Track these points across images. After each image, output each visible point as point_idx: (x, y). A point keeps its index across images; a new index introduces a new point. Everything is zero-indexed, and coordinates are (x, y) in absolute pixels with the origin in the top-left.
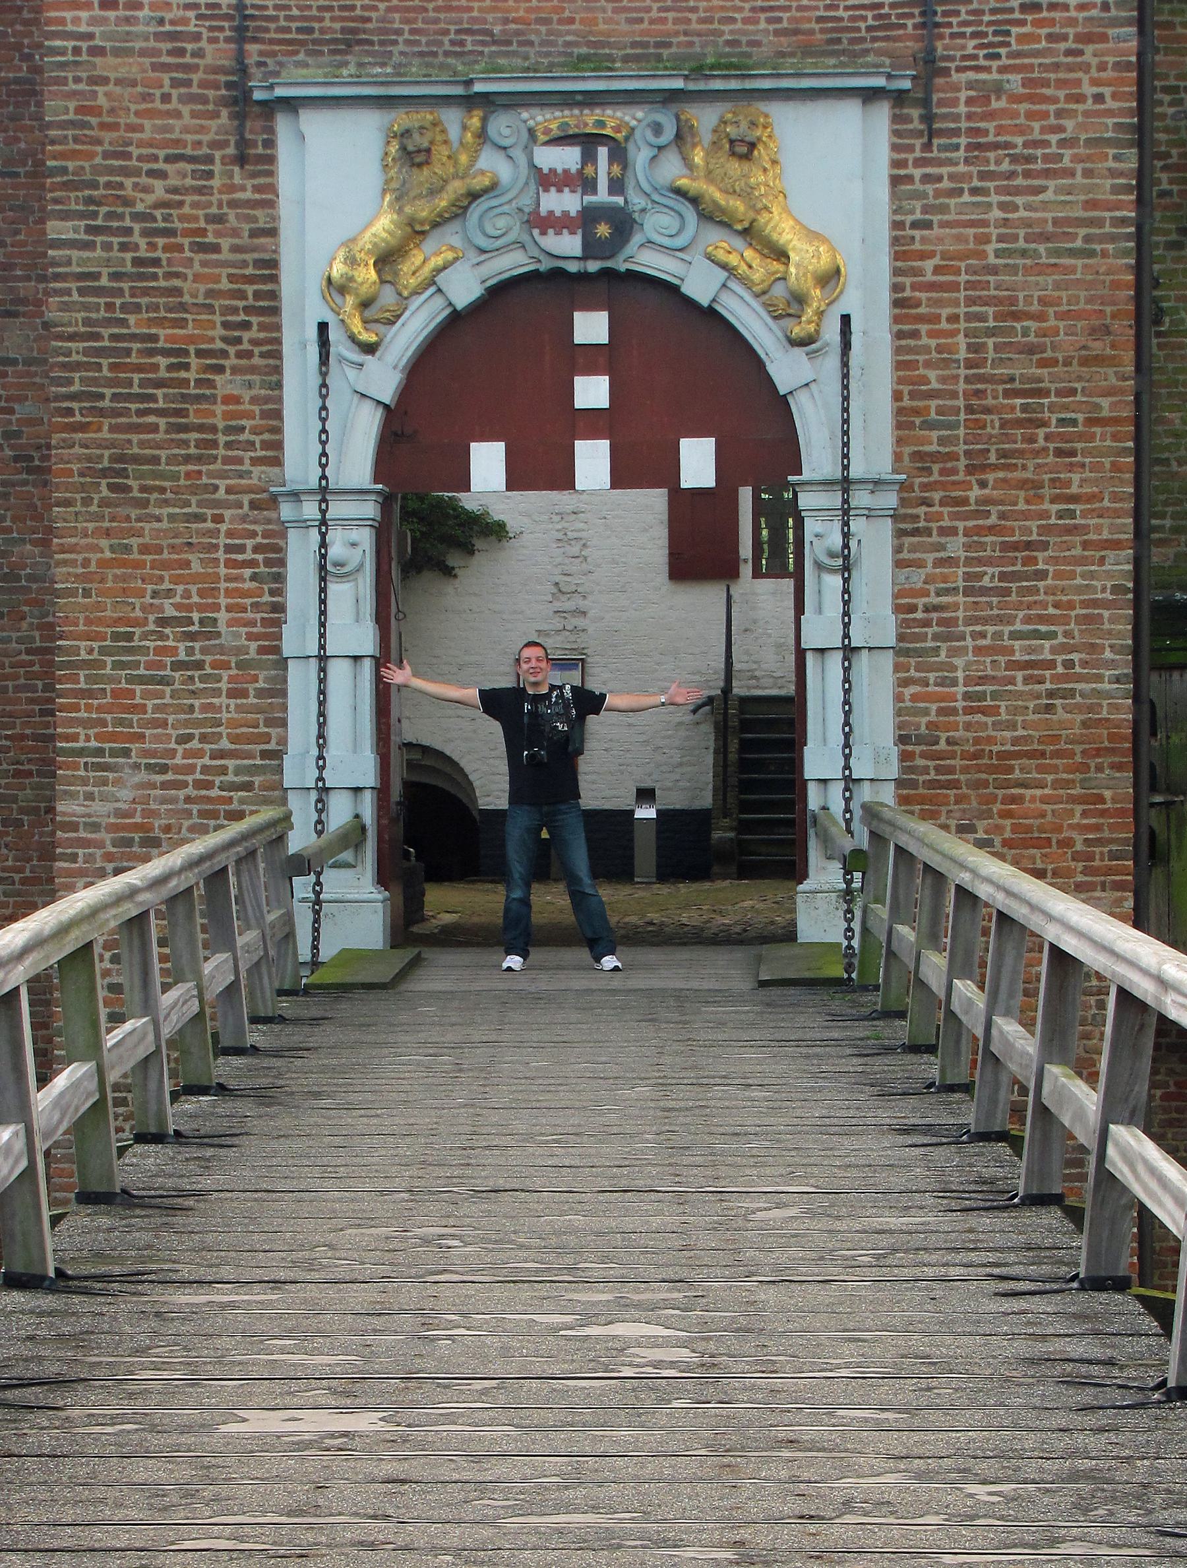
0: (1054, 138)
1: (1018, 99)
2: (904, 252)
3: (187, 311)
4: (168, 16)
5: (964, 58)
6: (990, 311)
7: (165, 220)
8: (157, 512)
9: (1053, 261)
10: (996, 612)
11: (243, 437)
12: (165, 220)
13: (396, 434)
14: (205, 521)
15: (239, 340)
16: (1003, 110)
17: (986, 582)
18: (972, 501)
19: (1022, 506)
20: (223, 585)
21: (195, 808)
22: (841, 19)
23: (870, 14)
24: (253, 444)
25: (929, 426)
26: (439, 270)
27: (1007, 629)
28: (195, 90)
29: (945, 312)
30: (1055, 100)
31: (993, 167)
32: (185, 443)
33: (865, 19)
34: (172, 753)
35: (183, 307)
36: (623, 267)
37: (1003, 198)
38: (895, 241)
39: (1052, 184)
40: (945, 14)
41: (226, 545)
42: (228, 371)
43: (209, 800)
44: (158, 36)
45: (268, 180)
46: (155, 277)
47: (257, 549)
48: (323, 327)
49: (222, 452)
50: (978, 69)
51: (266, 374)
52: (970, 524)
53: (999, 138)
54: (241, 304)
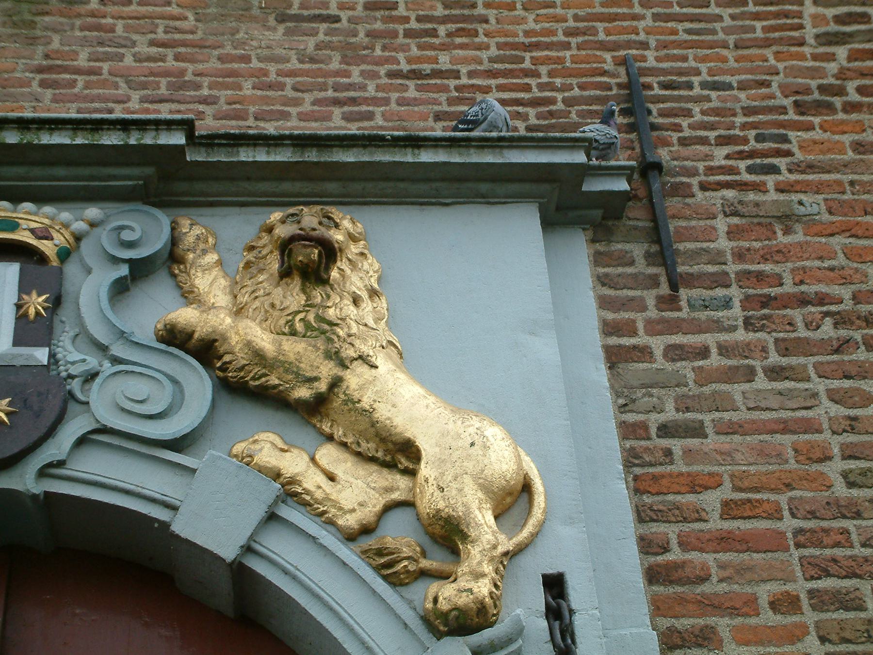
2: (655, 478)
5: (710, 170)
16: (800, 244)
23: (532, 112)
29: (765, 592)
31: (803, 333)
37: (836, 384)
40: (662, 114)
50: (743, 186)
53: (803, 288)
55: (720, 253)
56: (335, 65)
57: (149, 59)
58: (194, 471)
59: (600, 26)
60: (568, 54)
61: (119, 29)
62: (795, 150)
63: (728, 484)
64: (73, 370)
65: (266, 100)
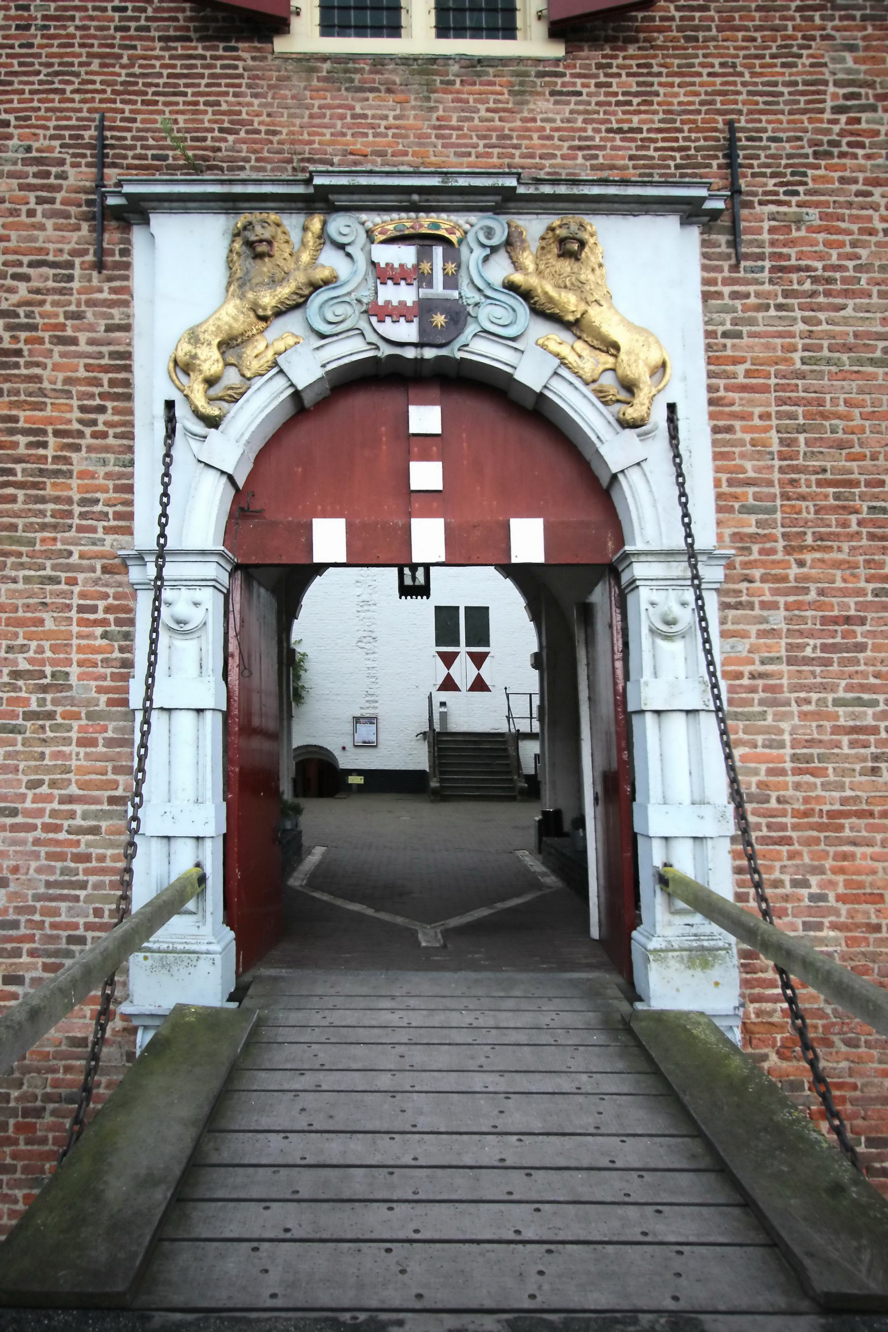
0: (850, 264)
1: (819, 230)
2: (718, 358)
3: (46, 396)
4: (36, 145)
5: (765, 193)
6: (800, 410)
7: (27, 316)
8: (13, 573)
9: (856, 368)
10: (819, 680)
11: (99, 508)
12: (27, 316)
13: (242, 509)
14: (59, 583)
15: (94, 423)
16: (803, 238)
17: (808, 652)
18: (792, 578)
19: (839, 584)
20: (75, 642)
21: (43, 850)
22: (653, 158)
23: (677, 155)
24: (107, 514)
25: (747, 510)
27: (830, 697)
28: (58, 206)
29: (757, 411)
30: (849, 232)
31: (796, 287)
32: (42, 513)
34: (23, 798)
35: (42, 393)
36: (459, 355)
38: (709, 347)
39: (850, 303)
40: (746, 157)
41: (79, 606)
42: (84, 449)
43: (58, 842)
44: (26, 162)
45: (125, 283)
46: (17, 366)
47: (107, 610)
49: (76, 521)
51: (120, 453)
52: (791, 599)
53: (800, 262)
54: (96, 390)
55: (763, 242)
56: (579, 124)
57: (487, 120)
58: (523, 352)
59: (718, 99)
60: (699, 117)
61: (471, 101)
62: (809, 180)
63: (749, 362)
64: (470, 302)
65: (543, 146)
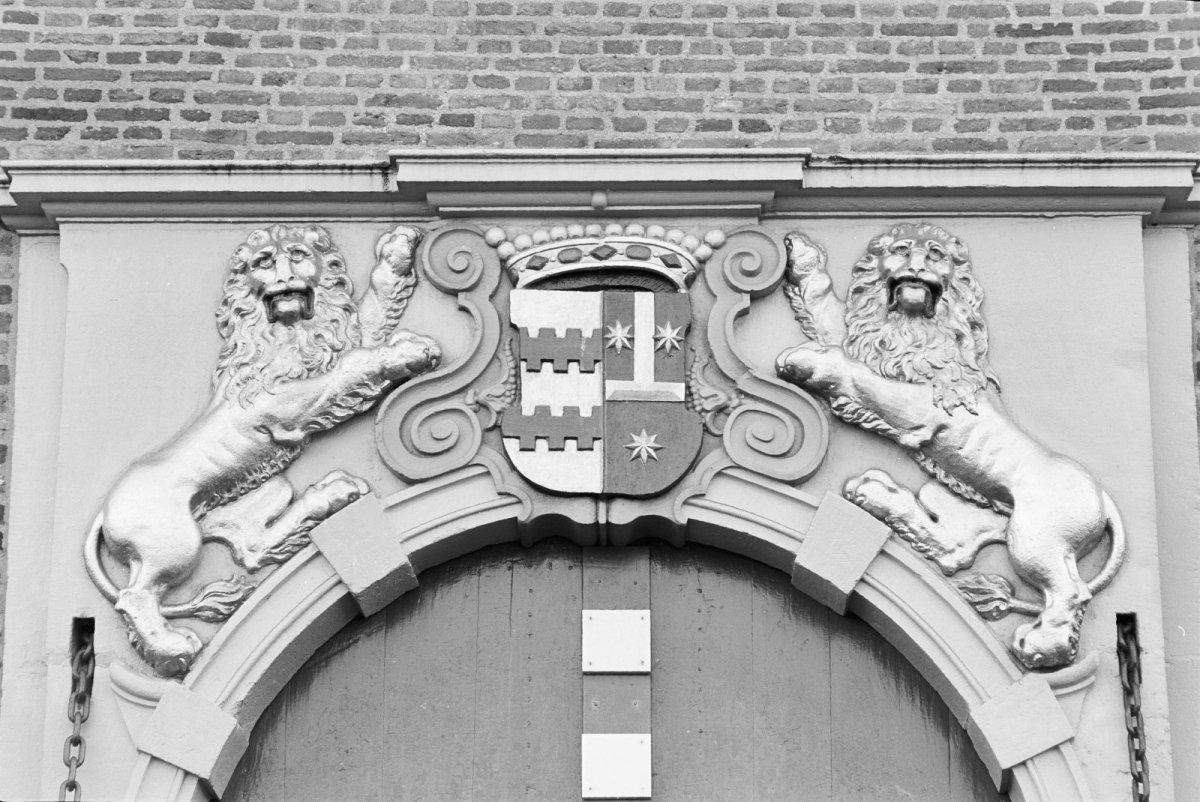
26: (319, 518)
33: (1134, 85)
36: (682, 516)
48: (84, 629)
58: (817, 508)
